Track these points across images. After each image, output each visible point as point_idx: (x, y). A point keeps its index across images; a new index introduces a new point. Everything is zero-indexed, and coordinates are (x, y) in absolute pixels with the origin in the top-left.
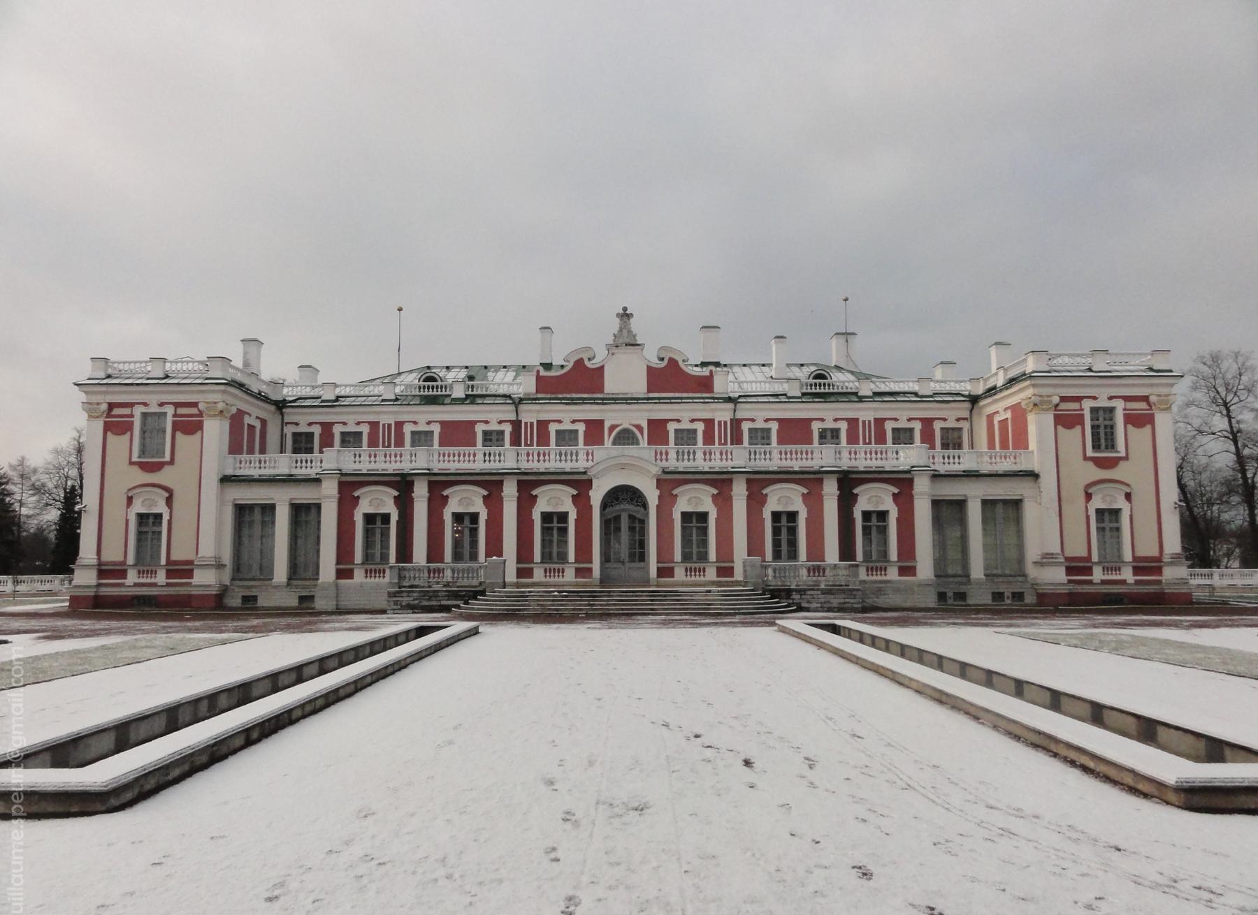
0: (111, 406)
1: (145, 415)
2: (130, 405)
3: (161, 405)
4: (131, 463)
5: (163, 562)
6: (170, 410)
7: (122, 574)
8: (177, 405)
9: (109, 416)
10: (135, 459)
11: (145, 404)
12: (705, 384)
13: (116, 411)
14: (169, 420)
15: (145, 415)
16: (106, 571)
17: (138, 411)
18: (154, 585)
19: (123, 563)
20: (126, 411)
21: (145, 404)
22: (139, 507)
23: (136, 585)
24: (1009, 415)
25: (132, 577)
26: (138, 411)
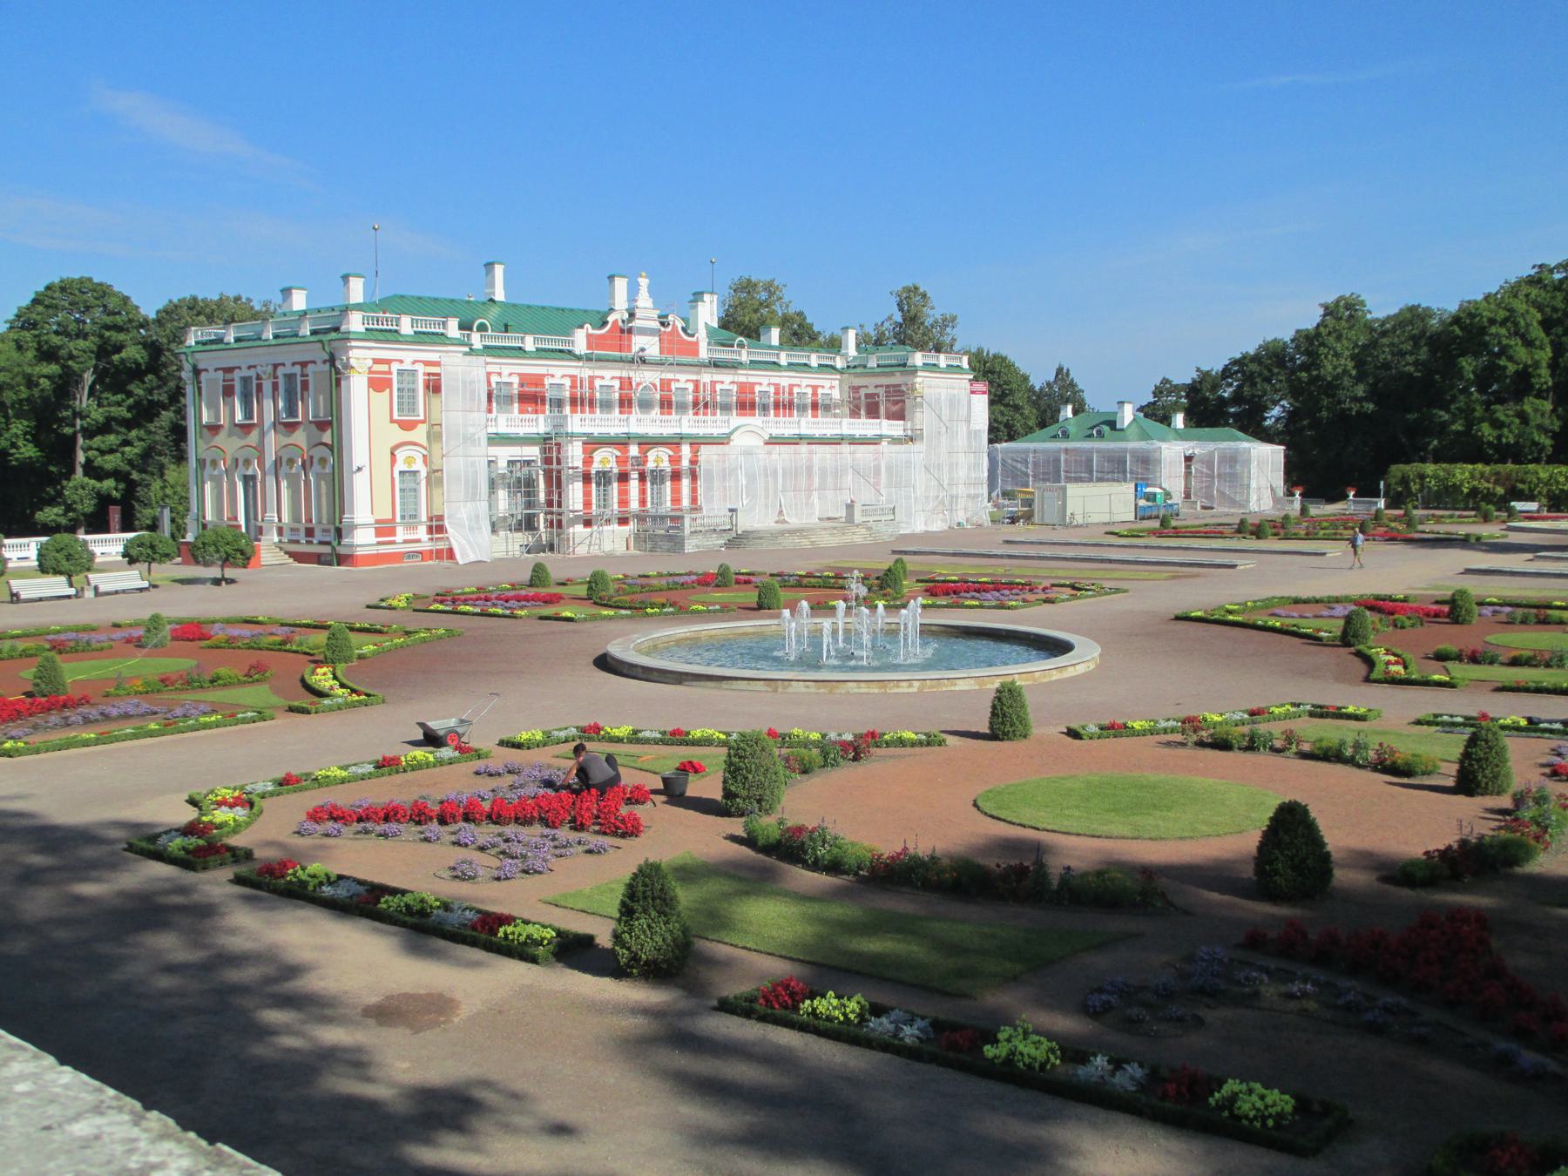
0: (376, 361)
1: (400, 372)
2: (388, 362)
3: (414, 362)
4: (392, 421)
5: (424, 518)
6: (421, 369)
7: (392, 532)
8: (427, 363)
9: (370, 372)
10: (396, 417)
11: (401, 362)
12: (693, 349)
13: (377, 368)
14: (421, 379)
15: (400, 372)
16: (384, 529)
17: (395, 367)
18: (418, 541)
19: (393, 519)
20: (384, 368)
21: (401, 362)
22: (400, 466)
23: (406, 542)
24: (881, 391)
25: (401, 534)
26: (395, 367)
